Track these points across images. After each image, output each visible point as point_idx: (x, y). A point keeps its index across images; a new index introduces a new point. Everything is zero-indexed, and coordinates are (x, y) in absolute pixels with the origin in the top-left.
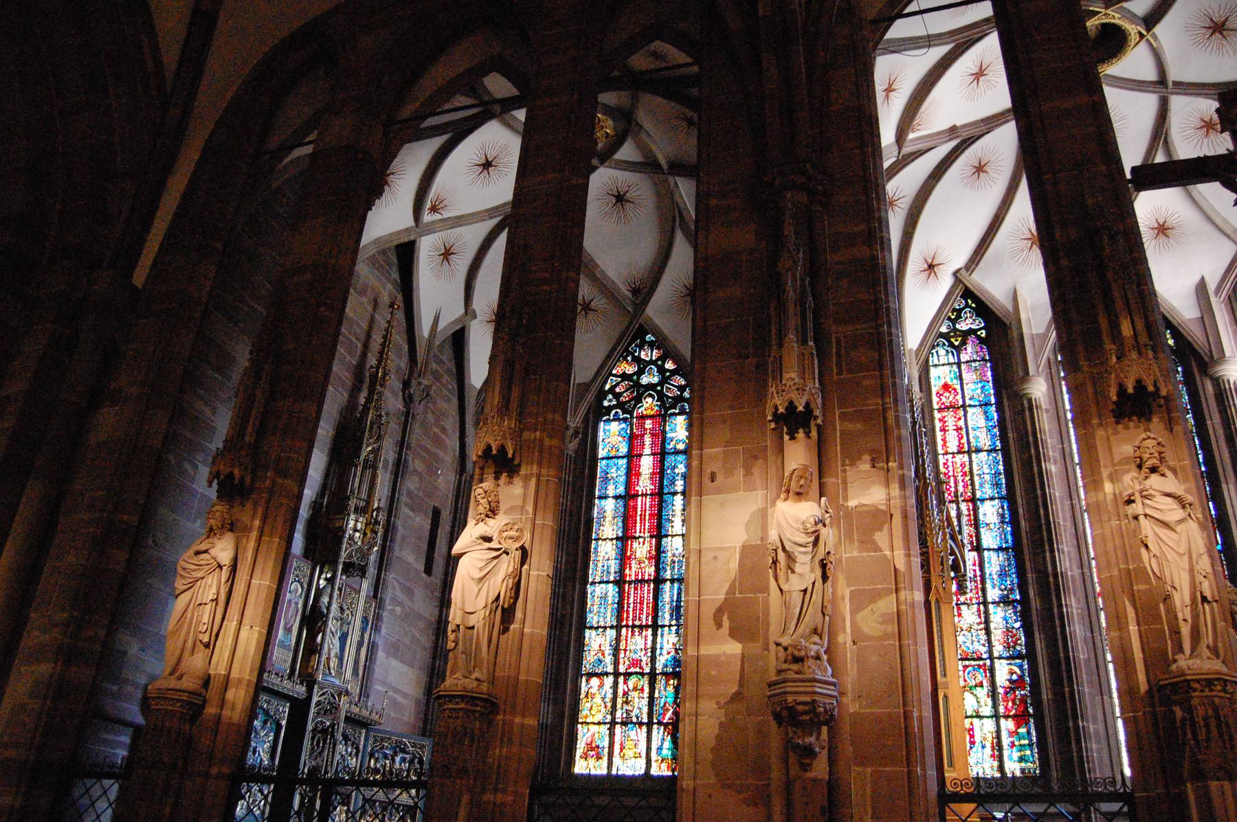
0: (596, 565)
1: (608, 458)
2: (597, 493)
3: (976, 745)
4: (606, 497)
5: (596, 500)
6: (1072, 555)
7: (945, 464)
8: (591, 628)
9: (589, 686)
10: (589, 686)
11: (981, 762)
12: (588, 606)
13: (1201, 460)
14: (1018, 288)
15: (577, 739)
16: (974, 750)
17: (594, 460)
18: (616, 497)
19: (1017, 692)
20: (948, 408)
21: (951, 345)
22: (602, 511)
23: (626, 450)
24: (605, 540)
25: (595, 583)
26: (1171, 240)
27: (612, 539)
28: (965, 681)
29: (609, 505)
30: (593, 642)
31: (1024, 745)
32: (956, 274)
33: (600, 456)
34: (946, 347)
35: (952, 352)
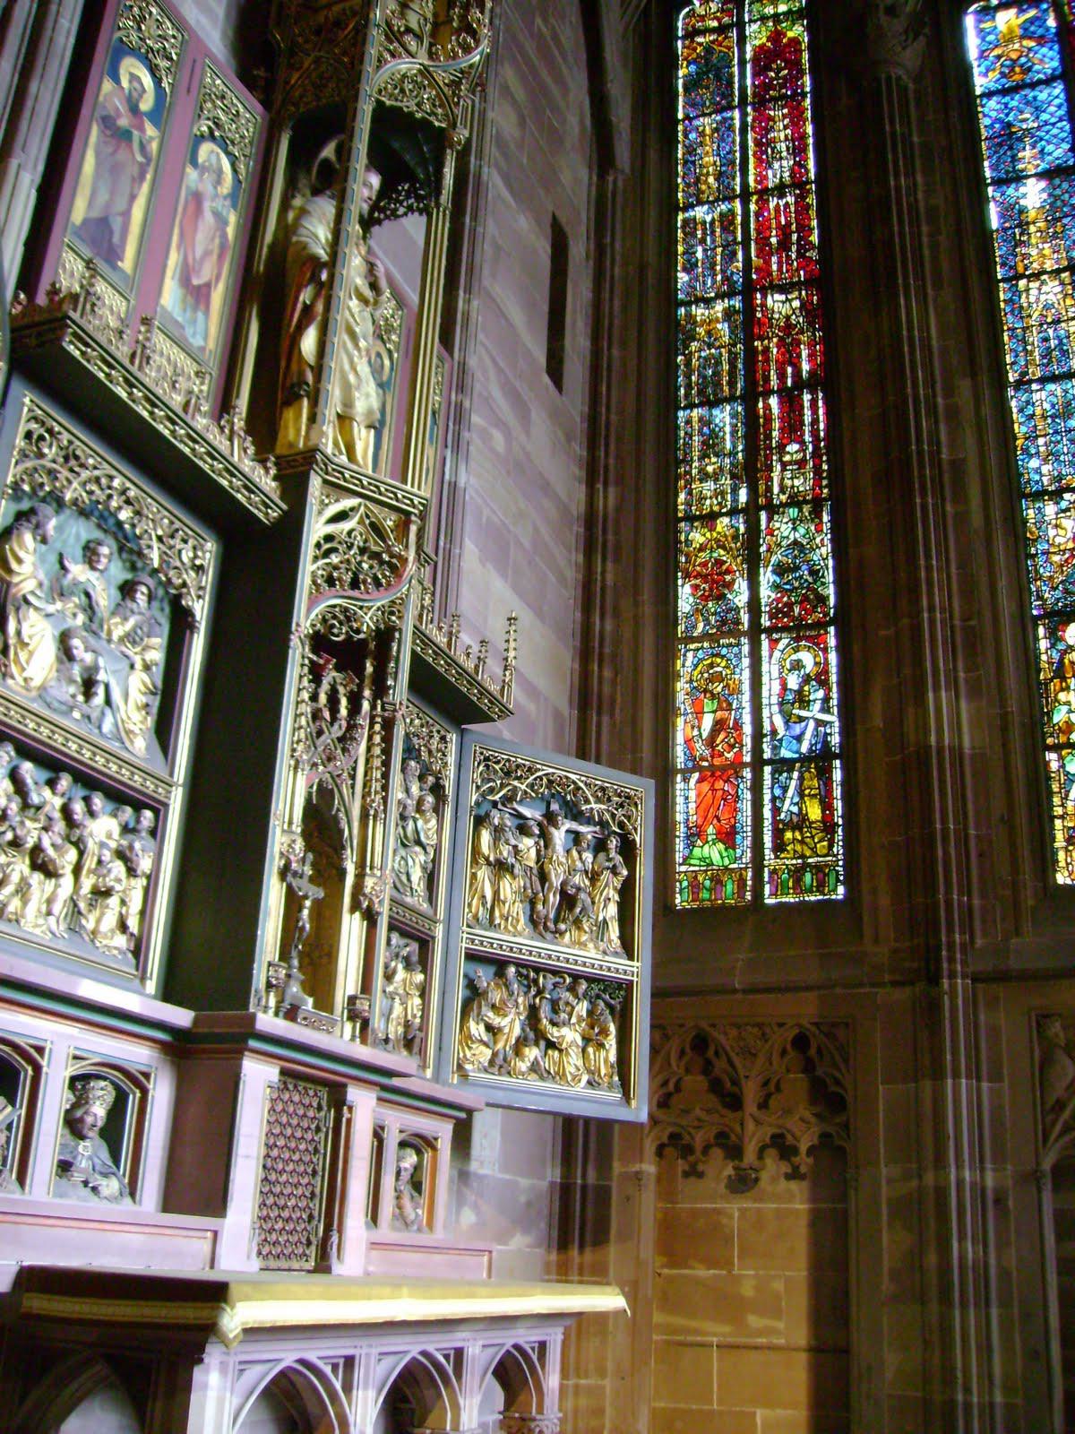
0: (1024, 341)
1: (1004, 92)
2: (988, 174)
4: (1018, 178)
5: (990, 189)
8: (1040, 495)
9: (1061, 646)
10: (1061, 646)
12: (1019, 442)
15: (1050, 794)
17: (967, 103)
18: (1046, 175)
22: (1015, 214)
23: (1055, 64)
24: (1036, 276)
25: (1030, 382)
27: (1057, 272)
29: (1033, 195)
30: (1052, 532)
33: (978, 91)
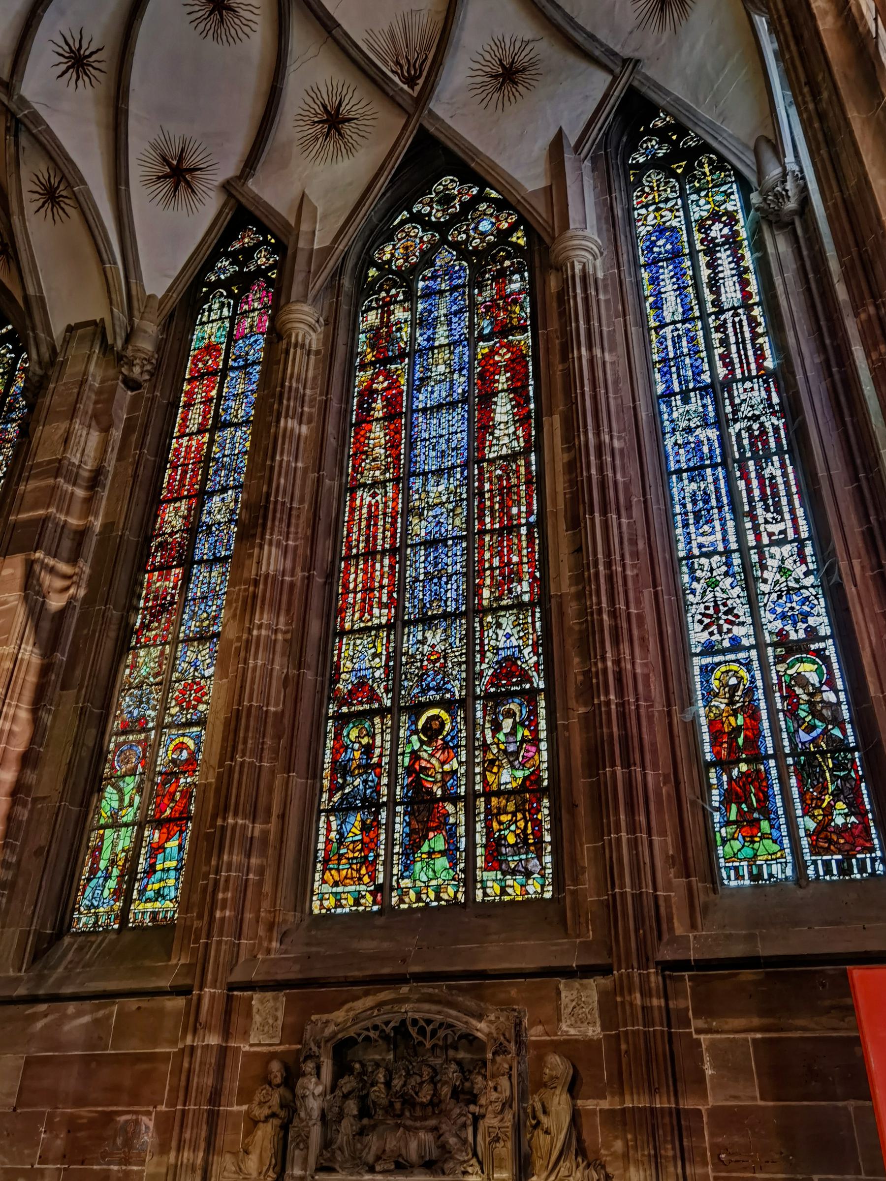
3: (99, 874)
6: (300, 551)
7: (176, 450)
11: (96, 903)
13: (531, 394)
14: (307, 192)
16: (93, 883)
19: (182, 780)
20: (202, 376)
21: (230, 295)
26: (520, 88)
28: (113, 767)
31: (169, 869)
32: (227, 187)
34: (222, 299)
35: (229, 303)
